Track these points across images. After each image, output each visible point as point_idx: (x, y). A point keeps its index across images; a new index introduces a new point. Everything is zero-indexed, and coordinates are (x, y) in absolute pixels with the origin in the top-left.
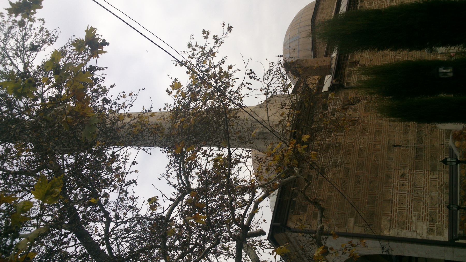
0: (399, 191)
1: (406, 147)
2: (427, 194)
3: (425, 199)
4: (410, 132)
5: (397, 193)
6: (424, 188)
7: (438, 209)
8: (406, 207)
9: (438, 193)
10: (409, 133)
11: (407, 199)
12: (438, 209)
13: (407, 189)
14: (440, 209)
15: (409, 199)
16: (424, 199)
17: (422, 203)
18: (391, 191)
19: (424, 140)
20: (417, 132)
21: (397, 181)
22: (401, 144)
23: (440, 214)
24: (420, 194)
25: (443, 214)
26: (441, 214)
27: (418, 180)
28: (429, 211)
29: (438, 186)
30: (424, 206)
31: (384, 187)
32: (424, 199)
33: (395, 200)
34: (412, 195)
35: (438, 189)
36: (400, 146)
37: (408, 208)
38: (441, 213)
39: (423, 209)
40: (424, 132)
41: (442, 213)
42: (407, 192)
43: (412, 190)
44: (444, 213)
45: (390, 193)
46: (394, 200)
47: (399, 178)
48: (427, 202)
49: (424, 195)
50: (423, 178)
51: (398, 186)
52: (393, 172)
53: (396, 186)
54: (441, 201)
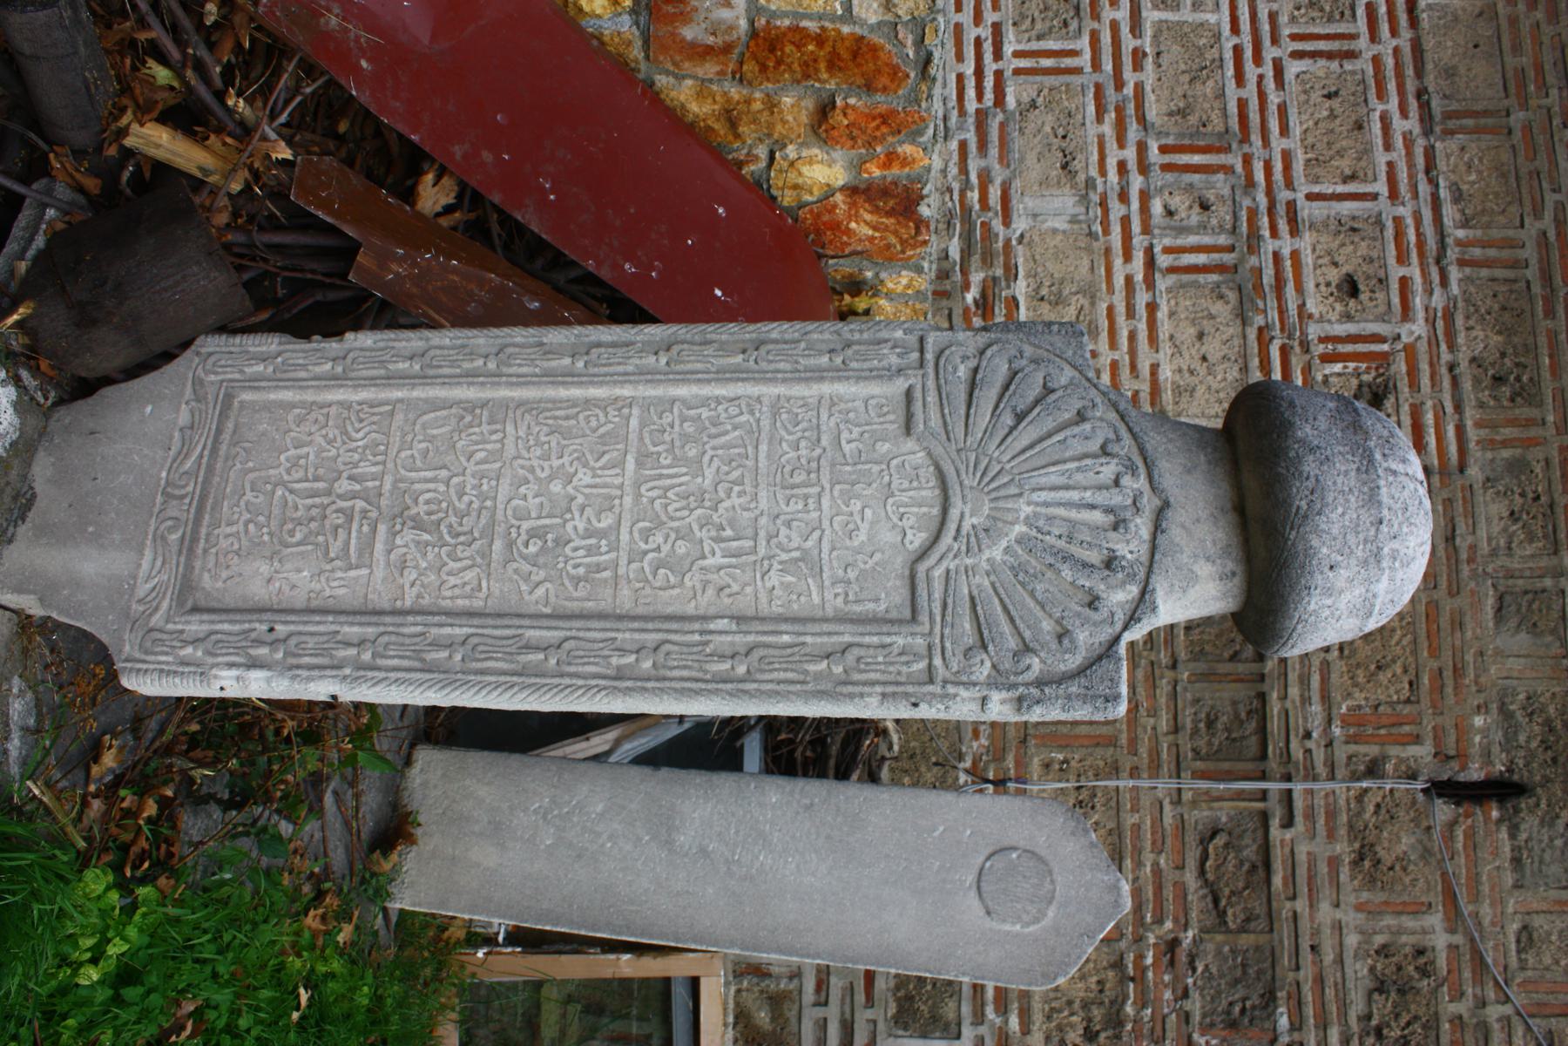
0: (1379, 223)
1: (1373, 770)
2: (1117, 210)
3: (1130, 154)
4: (1357, 1007)
5: (1394, 195)
6: (1150, 263)
7: (1010, 64)
8: (1293, 68)
9: (1020, 224)
10: (1358, 971)
11: (1293, 143)
12: (1010, 64)
13: (1305, 242)
14: (990, 66)
15: (1278, 144)
16: (1142, 148)
17: (1152, 113)
18: (1449, 213)
19: (1190, 878)
20: (1270, 998)
21: (1418, 328)
22: (1443, 811)
23: (990, 17)
24: (1179, 202)
25: (966, 17)
26: (978, 19)
27: (1213, 348)
28: (1084, 43)
29: (1021, 288)
30: (1129, 76)
31: (1530, 253)
32: (1142, 148)
33: (1399, 125)
34: (1250, 183)
35: (1021, 257)
36: (1445, 789)
37: (1270, 53)
38: (985, 32)
39: (1138, 56)
40: (1195, 1005)
41: (971, 33)
42: (1306, 210)
43: (1254, 238)
44: (958, 27)
45: (1458, 196)
46: (1413, 124)
47: (1400, 366)
48: (1107, 128)
49: (1145, 197)
50: (1166, 373)
51: (1396, 272)
52: (1472, 434)
53: (1415, 272)
54: (983, 146)
